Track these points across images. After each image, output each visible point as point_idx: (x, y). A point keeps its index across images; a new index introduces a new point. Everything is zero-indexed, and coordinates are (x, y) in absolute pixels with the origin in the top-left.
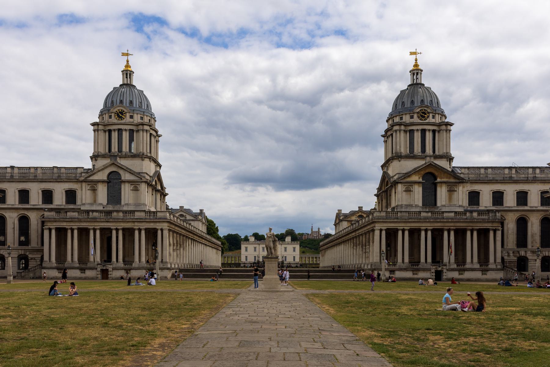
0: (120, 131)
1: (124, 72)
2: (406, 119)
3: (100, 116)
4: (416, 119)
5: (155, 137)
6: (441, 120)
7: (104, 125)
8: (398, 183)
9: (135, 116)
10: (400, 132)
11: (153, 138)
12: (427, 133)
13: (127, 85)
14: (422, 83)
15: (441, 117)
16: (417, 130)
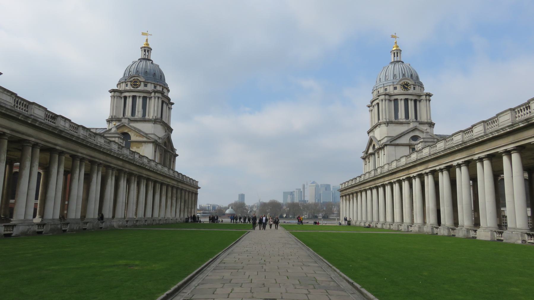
0: (134, 97)
1: (143, 49)
2: (390, 90)
3: (118, 85)
4: (399, 90)
5: (167, 104)
6: (421, 91)
7: (121, 92)
8: (386, 145)
9: (149, 85)
10: (385, 100)
11: (165, 105)
12: (409, 102)
13: (144, 59)
14: (402, 60)
15: (420, 89)
16: (401, 100)
